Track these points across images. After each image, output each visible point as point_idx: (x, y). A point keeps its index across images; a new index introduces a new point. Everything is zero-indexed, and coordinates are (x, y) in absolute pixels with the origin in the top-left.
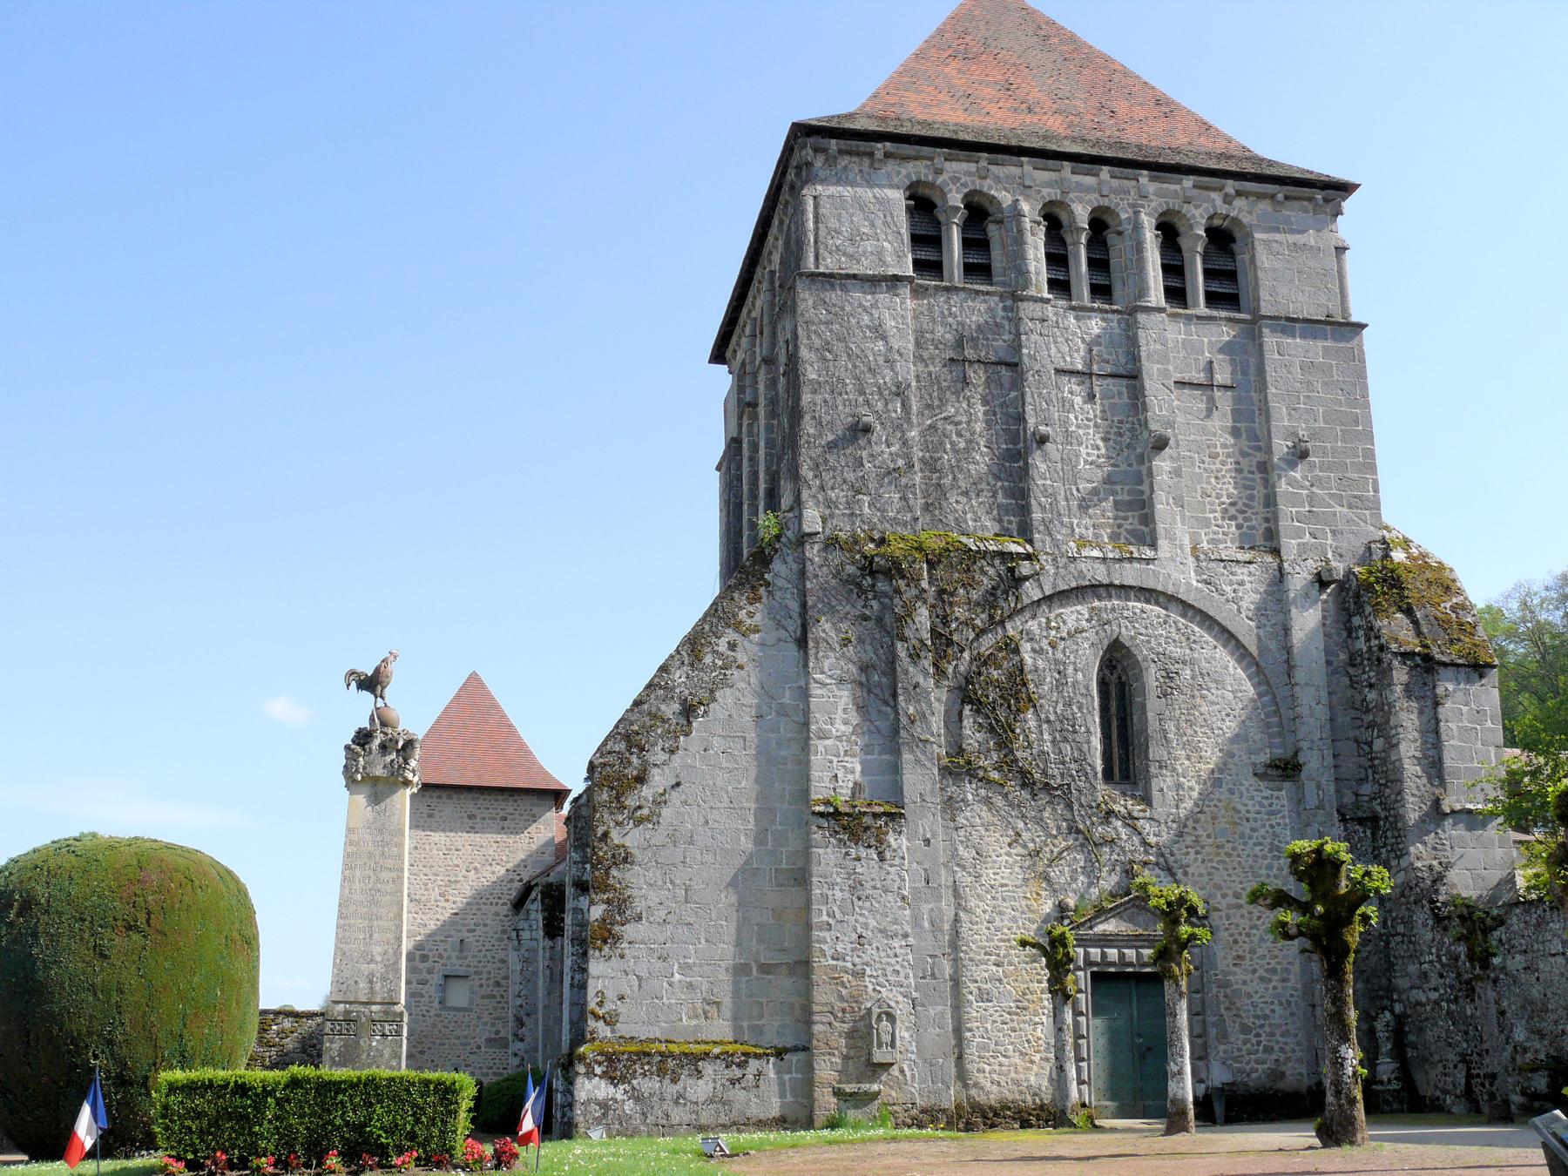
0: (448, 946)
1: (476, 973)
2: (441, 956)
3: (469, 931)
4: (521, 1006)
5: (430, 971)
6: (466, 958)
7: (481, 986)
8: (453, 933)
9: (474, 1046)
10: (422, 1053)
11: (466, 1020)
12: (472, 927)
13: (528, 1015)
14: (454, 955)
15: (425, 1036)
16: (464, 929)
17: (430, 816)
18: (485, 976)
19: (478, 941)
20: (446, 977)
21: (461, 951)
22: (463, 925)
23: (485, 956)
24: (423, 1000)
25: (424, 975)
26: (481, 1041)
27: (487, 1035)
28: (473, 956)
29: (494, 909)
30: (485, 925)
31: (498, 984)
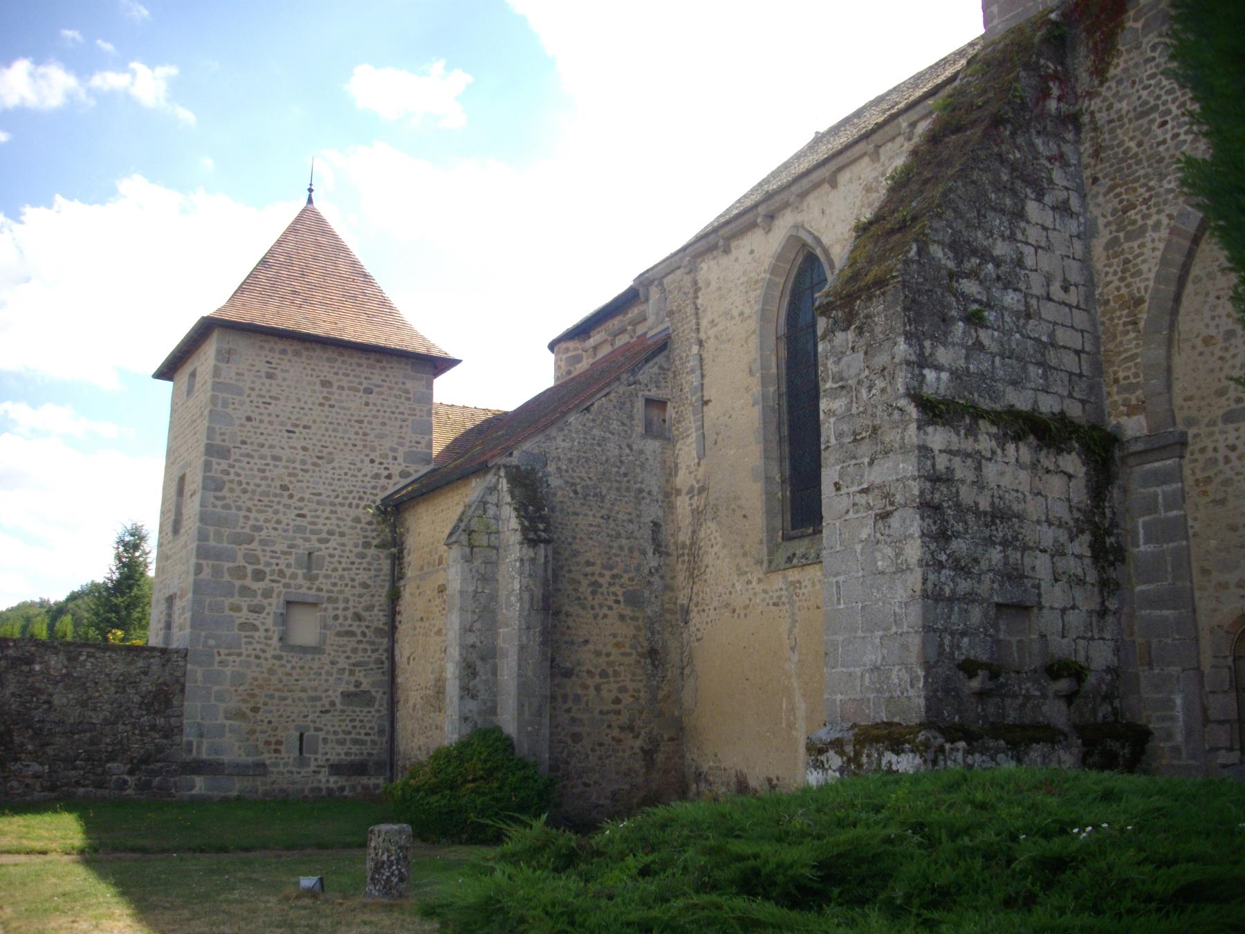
0: (292, 560)
1: (330, 600)
2: (281, 573)
3: (321, 541)
4: (473, 646)
5: (267, 594)
6: (316, 577)
7: (336, 617)
8: (299, 542)
9: (326, 702)
10: (255, 710)
11: (316, 665)
12: (324, 535)
13: (483, 659)
14: (300, 572)
15: (260, 687)
16: (314, 537)
17: (270, 376)
18: (341, 605)
19: (332, 556)
20: (289, 603)
21: (309, 568)
22: (312, 532)
23: (342, 577)
24: (256, 634)
25: (259, 600)
28: (327, 577)
29: (353, 513)
30: (342, 534)
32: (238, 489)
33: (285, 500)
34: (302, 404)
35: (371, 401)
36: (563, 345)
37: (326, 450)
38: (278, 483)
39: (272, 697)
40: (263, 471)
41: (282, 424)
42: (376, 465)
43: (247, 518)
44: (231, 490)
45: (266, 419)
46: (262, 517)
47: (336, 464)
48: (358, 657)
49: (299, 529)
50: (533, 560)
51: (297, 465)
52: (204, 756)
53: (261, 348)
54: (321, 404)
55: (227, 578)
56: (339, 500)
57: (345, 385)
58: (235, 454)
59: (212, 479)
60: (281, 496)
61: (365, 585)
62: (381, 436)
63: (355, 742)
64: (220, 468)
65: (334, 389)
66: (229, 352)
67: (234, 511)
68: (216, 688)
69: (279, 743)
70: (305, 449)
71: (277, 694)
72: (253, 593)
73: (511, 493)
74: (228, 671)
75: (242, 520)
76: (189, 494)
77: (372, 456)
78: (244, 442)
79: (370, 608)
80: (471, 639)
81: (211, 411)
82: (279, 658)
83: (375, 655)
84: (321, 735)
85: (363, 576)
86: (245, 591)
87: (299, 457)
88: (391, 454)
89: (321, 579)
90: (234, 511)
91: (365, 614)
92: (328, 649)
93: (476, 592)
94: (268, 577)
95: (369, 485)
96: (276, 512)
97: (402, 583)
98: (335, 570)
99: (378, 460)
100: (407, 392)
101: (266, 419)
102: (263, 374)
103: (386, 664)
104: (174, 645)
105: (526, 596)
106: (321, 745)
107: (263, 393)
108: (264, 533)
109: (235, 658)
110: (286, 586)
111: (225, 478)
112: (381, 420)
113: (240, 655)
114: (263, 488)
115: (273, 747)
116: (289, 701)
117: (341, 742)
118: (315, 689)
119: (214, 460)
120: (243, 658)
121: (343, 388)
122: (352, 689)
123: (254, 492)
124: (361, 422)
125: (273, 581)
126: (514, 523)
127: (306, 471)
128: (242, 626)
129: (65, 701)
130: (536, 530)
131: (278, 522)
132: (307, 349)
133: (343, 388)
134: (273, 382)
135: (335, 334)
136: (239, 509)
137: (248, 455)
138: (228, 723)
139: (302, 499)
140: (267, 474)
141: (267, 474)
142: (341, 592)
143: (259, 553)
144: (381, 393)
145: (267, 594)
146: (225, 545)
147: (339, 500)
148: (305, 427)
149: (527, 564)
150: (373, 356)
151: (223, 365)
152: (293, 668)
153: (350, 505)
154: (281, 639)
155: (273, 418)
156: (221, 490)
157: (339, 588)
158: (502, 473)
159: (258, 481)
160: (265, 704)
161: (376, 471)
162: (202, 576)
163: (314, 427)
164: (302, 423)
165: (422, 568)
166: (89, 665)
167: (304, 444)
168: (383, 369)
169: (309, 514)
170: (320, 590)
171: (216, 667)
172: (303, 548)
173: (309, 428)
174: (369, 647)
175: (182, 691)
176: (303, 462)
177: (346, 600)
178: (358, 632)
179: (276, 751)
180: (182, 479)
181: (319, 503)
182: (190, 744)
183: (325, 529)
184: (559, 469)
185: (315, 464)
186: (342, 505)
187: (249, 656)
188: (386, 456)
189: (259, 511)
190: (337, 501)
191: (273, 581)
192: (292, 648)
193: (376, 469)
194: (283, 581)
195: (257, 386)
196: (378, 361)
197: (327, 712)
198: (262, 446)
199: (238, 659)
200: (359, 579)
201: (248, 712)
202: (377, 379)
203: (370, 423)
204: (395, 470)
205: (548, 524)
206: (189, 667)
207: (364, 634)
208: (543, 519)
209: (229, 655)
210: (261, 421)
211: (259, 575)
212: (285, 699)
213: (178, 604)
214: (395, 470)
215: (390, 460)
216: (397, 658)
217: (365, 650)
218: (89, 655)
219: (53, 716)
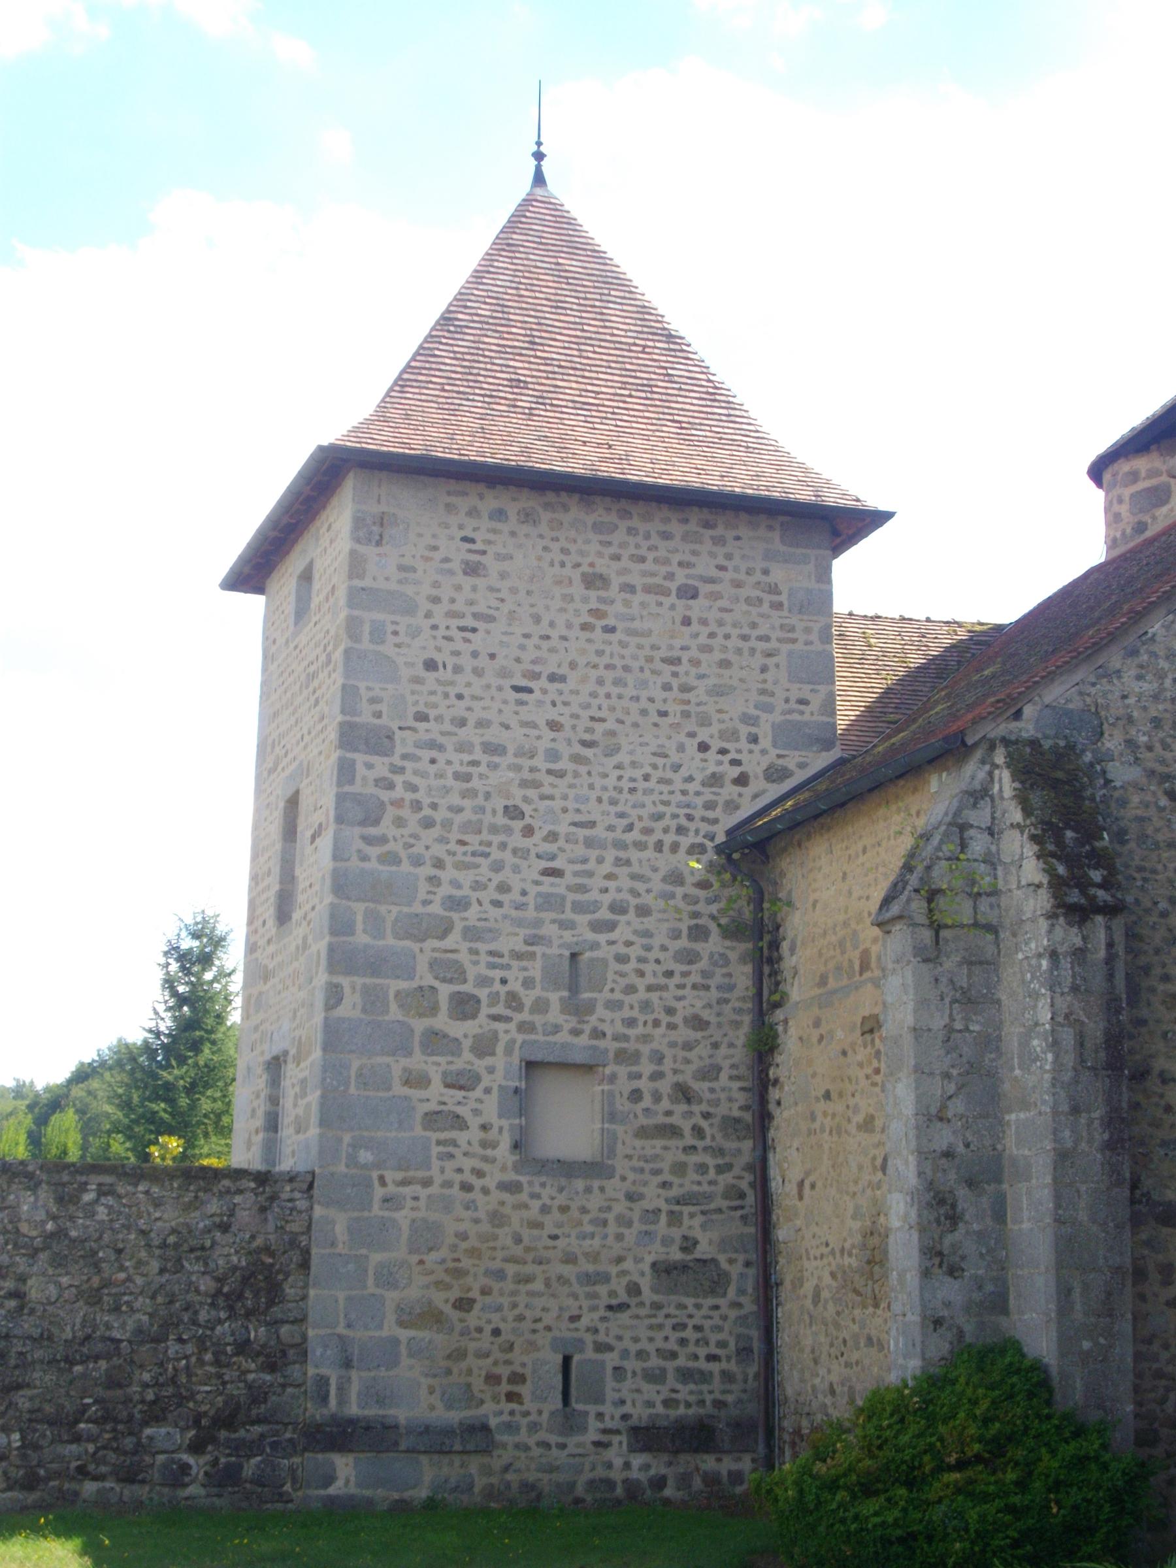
0: (536, 970)
1: (622, 1057)
2: (513, 1000)
3: (599, 926)
4: (948, 1154)
5: (484, 1046)
6: (590, 1008)
7: (636, 1096)
8: (549, 930)
10: (465, 1304)
11: (595, 1202)
12: (604, 914)
13: (971, 1183)
14: (554, 997)
15: (473, 1253)
16: (582, 919)
17: (472, 570)
18: (647, 1068)
19: (622, 959)
20: (531, 1066)
21: (574, 988)
23: (646, 1006)
24: (462, 1137)
25: (466, 1059)
26: (640, 1271)
27: (654, 1252)
29: (666, 861)
30: (643, 911)
31: (684, 1093)
32: (413, 819)
33: (517, 840)
34: (544, 628)
35: (694, 615)
36: (1124, 467)
37: (600, 728)
38: (499, 803)
39: (500, 1275)
40: (467, 778)
41: (504, 673)
42: (712, 755)
43: (433, 880)
44: (399, 822)
45: (467, 662)
46: (466, 878)
47: (623, 757)
48: (689, 1183)
49: (548, 902)
50: (1079, 954)
51: (539, 762)
52: (354, 1409)
53: (449, 508)
54: (585, 627)
55: (395, 1013)
56: (635, 835)
57: (637, 580)
58: (404, 743)
59: (358, 799)
60: (508, 830)
61: (698, 1023)
62: (718, 692)
63: (686, 1375)
64: (372, 775)
65: (613, 591)
66: (381, 521)
67: (406, 867)
68: (376, 1257)
69: (517, 1378)
70: (554, 726)
71: (511, 1269)
72: (452, 1046)
73: (1023, 801)
74: (403, 1217)
75: (423, 887)
76: (309, 834)
77: (703, 735)
78: (422, 717)
79: (710, 1073)
80: (944, 1137)
81: (347, 652)
82: (512, 1187)
83: (726, 1179)
84: (611, 1359)
85: (693, 1003)
86: (435, 1041)
87: (543, 745)
88: (744, 730)
89: (600, 1011)
90: (406, 867)
91: (700, 1087)
92: (621, 1166)
93: (949, 1029)
94: (485, 1010)
95: (699, 801)
96: (497, 867)
97: (779, 1015)
98: (630, 989)
99: (716, 745)
100: (774, 590)
101: (467, 662)
102: (456, 565)
103: (750, 1199)
104: (286, 1165)
105: (1068, 1037)
106: (610, 1383)
107: (459, 606)
108: (473, 912)
109: (417, 1189)
110: (523, 1027)
111: (385, 795)
112: (718, 656)
113: (427, 1183)
114: (468, 815)
115: (505, 1387)
116: (538, 1285)
117: (654, 1377)
118: (594, 1257)
119: (360, 758)
120: (434, 1189)
121: (630, 588)
122: (677, 1256)
123: (447, 824)
124: (676, 661)
125: (496, 1018)
126: (1032, 870)
127: (561, 774)
128: (432, 1119)
129: (52, 1291)
130: (1084, 885)
131: (503, 888)
132: (548, 506)
133: (630, 588)
134: (480, 582)
135: (609, 470)
136: (417, 862)
137: (433, 745)
138: (404, 1334)
139: (552, 837)
140: (475, 783)
141: (475, 783)
142: (646, 1039)
143: (464, 957)
144: (716, 596)
145: (484, 1046)
146: (390, 941)
147: (635, 835)
148: (553, 678)
149: (1065, 963)
150: (696, 515)
151: (370, 551)
152: (545, 1210)
153: (659, 846)
154: (516, 1146)
155: (484, 661)
156: (376, 822)
157: (640, 1030)
158: (1000, 758)
159: (456, 800)
160: (485, 1292)
161: (712, 768)
162: (342, 1011)
163: (573, 678)
164: (547, 670)
165: (823, 981)
166: (102, 1213)
167: (552, 714)
168: (719, 541)
169: (569, 869)
170: (598, 1034)
171: (377, 1210)
172: (559, 942)
173: (563, 679)
174: (711, 1162)
175: (305, 1265)
176: (553, 755)
177: (659, 1058)
178: (686, 1126)
179: (511, 1397)
180: (293, 803)
181: (589, 843)
182: (323, 1382)
183: (607, 899)
184: (1130, 743)
185: (577, 759)
186: (640, 846)
187: (448, 1184)
188: (734, 735)
189: (461, 866)
190: (629, 837)
191: (496, 1018)
192: (544, 1166)
193: (713, 763)
194: (518, 1017)
195: (446, 593)
196: (707, 525)
197: (622, 1307)
198: (462, 723)
199: (423, 1193)
200: (683, 1010)
201: (448, 1309)
202: (705, 566)
203: (695, 663)
204: (755, 764)
205: (1112, 870)
206: (318, 1211)
207: (698, 1132)
208: (1099, 859)
209: (404, 1183)
210: (457, 669)
211: (464, 1006)
212: (528, 1279)
213: (293, 1074)
214: (755, 764)
215: (744, 744)
216: (775, 1185)
217: (702, 1168)
218: (103, 1191)
219: (28, 1325)
